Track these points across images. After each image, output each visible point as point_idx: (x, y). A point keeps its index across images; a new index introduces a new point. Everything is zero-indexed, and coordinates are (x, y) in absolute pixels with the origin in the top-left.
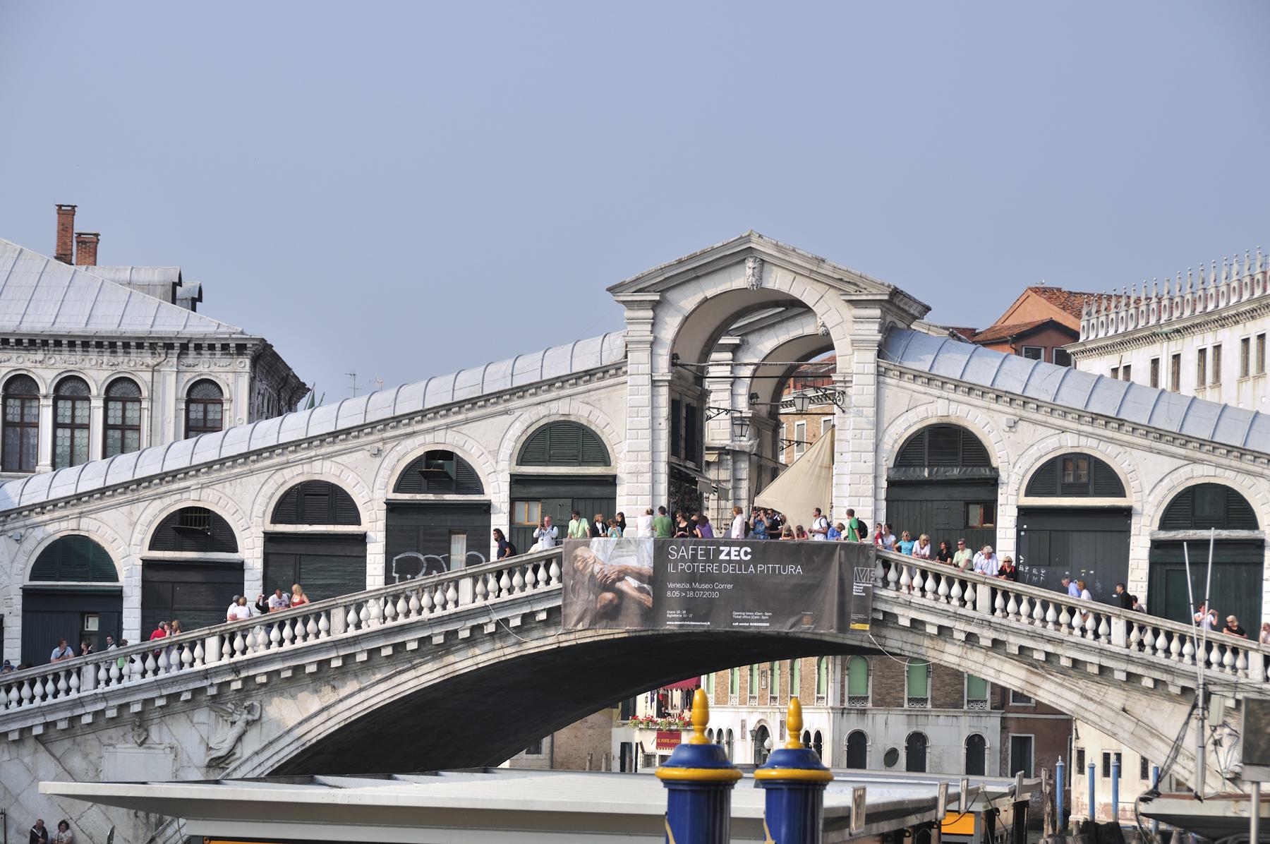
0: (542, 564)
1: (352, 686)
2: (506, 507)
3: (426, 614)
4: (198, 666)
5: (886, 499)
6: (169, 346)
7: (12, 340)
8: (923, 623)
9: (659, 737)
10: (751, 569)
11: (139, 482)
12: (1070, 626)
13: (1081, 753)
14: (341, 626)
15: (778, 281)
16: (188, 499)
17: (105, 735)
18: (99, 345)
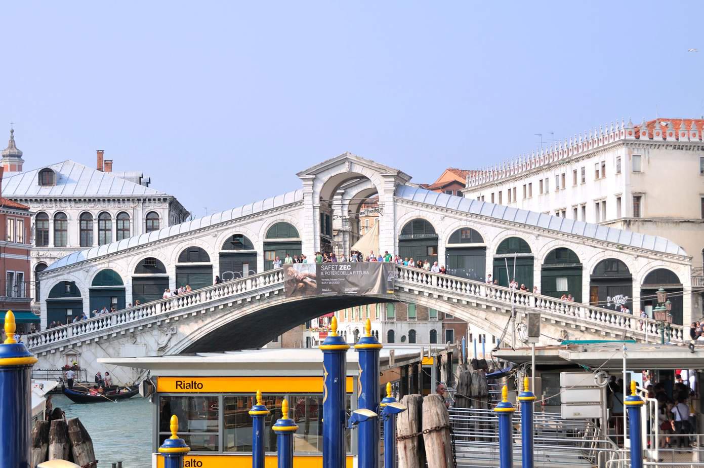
0: (276, 273)
1: (209, 320)
2: (262, 254)
3: (235, 293)
4: (153, 315)
5: (399, 246)
6: (139, 200)
7: (82, 200)
8: (413, 290)
9: (320, 334)
10: (351, 273)
11: (130, 249)
12: (466, 290)
13: (471, 335)
14: (205, 299)
15: (358, 170)
17: (121, 341)
18: (114, 200)
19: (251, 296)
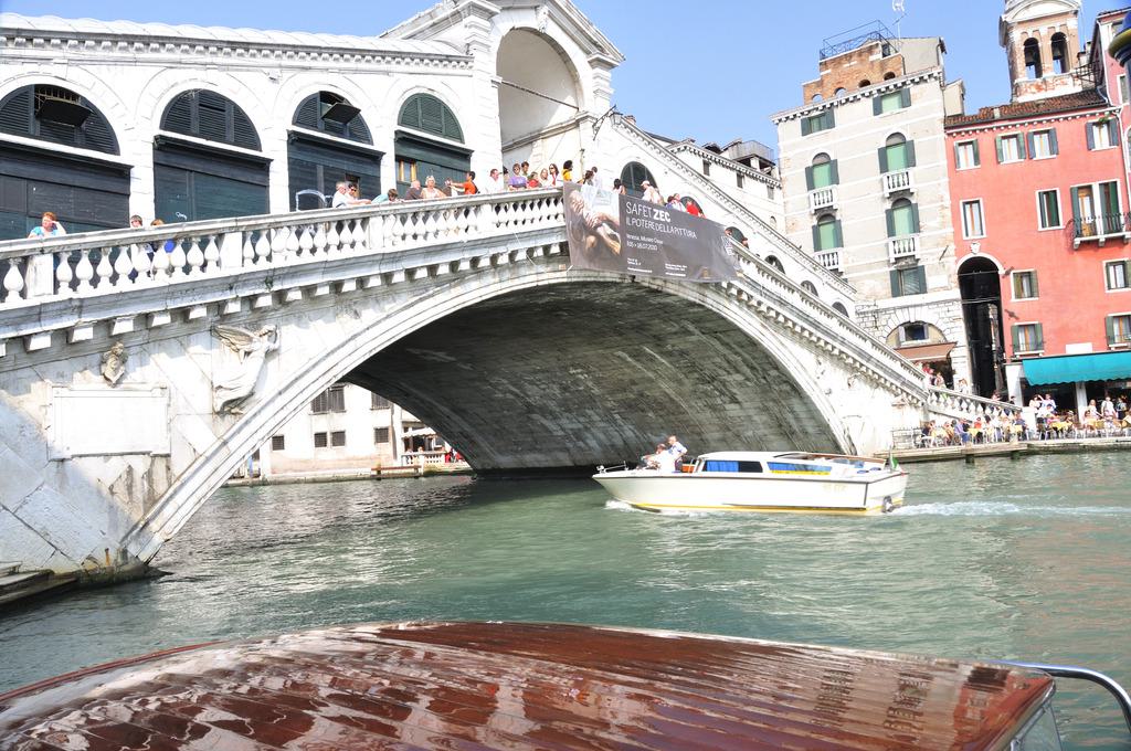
15: (553, 31)
16: (49, 75)
19: (493, 251)
